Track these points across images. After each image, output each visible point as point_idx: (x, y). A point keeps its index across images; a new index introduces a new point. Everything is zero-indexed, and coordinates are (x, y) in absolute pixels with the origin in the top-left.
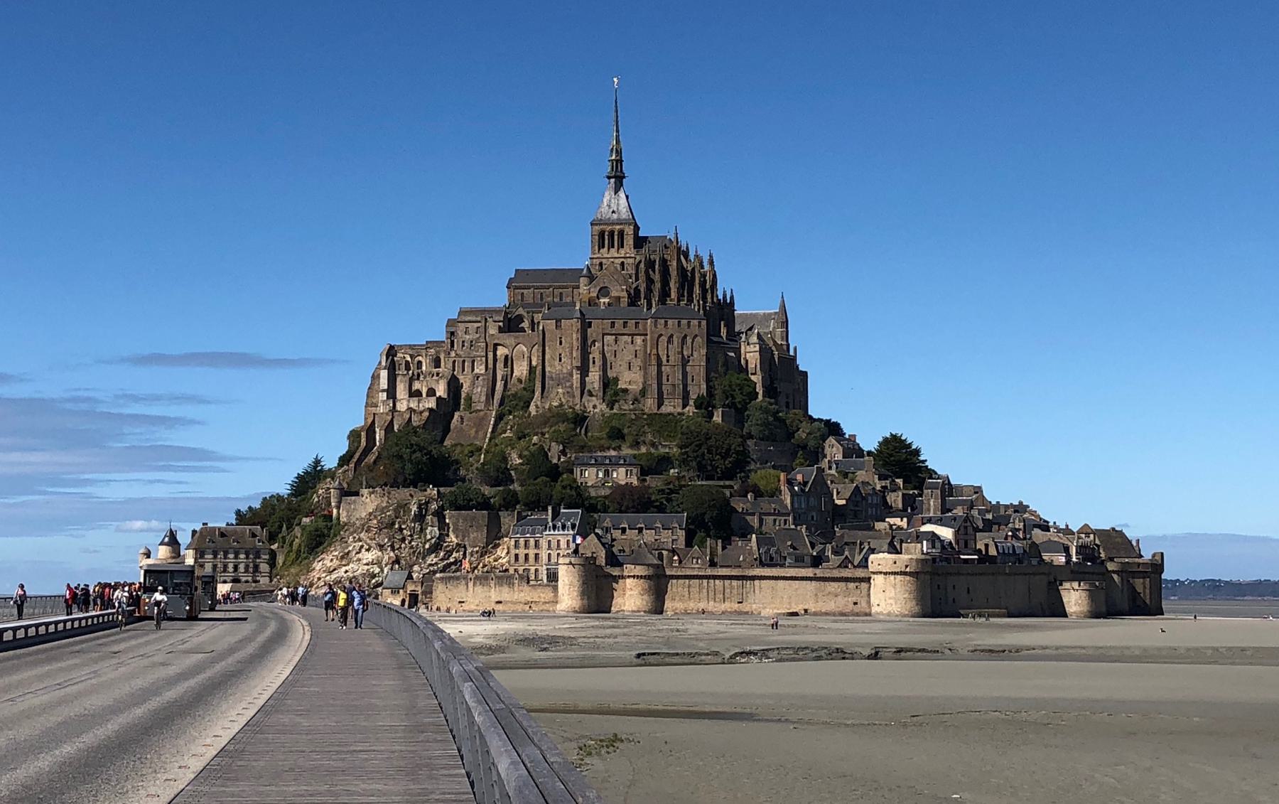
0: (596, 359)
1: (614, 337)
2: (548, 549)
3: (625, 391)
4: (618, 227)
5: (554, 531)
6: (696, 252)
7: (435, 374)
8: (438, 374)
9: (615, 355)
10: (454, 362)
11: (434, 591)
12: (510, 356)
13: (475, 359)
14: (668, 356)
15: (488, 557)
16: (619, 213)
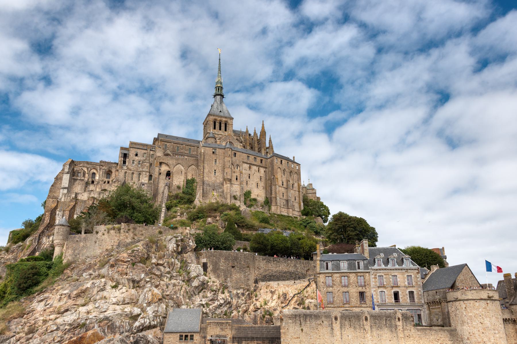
0: (238, 177)
1: (248, 165)
2: (379, 287)
3: (255, 200)
4: (224, 119)
5: (385, 266)
6: (270, 138)
7: (107, 182)
8: (108, 182)
9: (249, 177)
10: (126, 173)
11: (282, 335)
12: (171, 171)
13: (141, 173)
14: (283, 182)
15: (257, 300)
16: (224, 113)
